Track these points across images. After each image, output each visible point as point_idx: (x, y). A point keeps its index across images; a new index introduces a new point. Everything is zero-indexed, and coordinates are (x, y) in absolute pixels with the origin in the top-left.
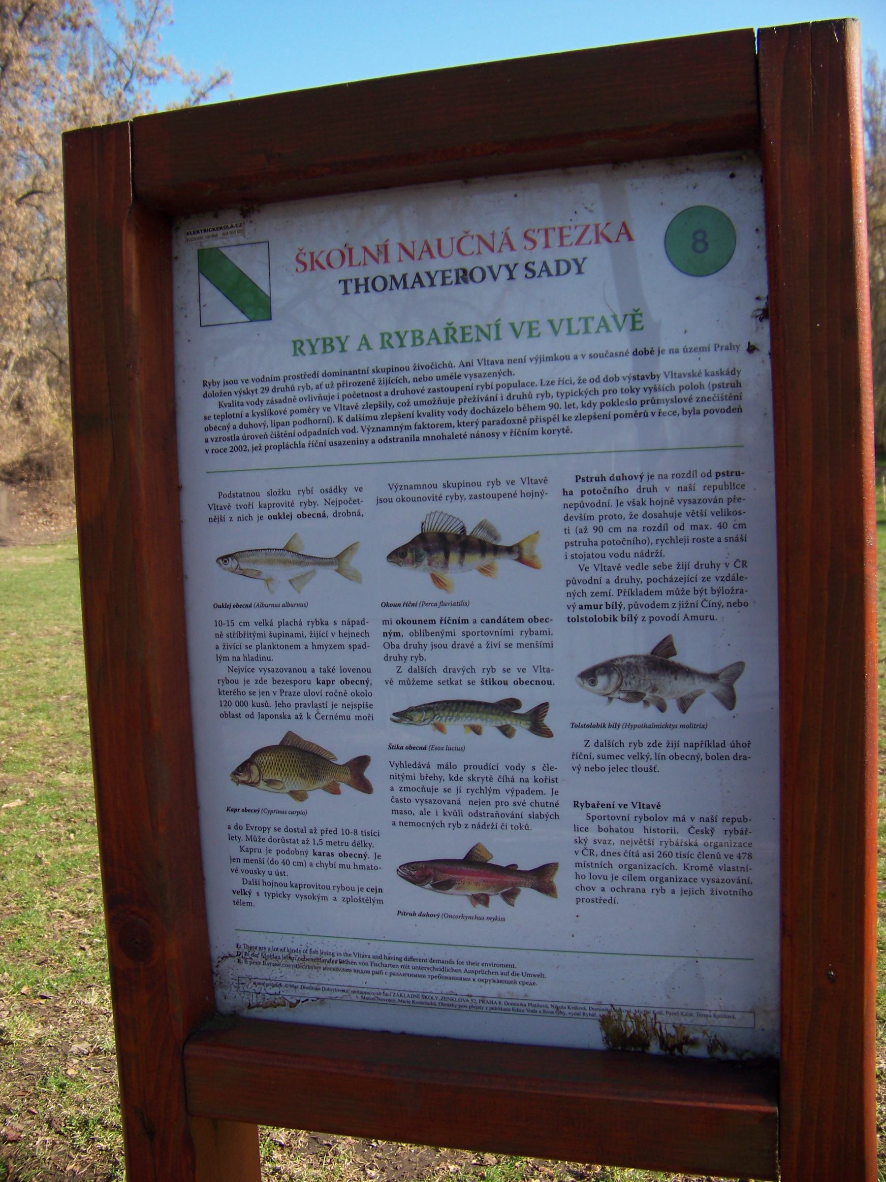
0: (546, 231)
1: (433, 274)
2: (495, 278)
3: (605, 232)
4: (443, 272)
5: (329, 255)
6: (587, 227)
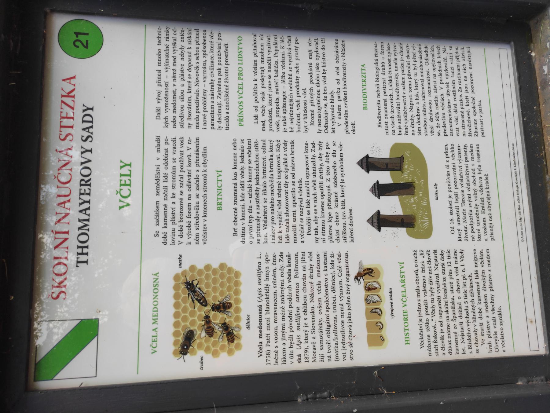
0: (61, 127)
1: (81, 201)
2: (89, 161)
3: (68, 91)
4: (81, 194)
5: (56, 275)
6: (62, 102)
